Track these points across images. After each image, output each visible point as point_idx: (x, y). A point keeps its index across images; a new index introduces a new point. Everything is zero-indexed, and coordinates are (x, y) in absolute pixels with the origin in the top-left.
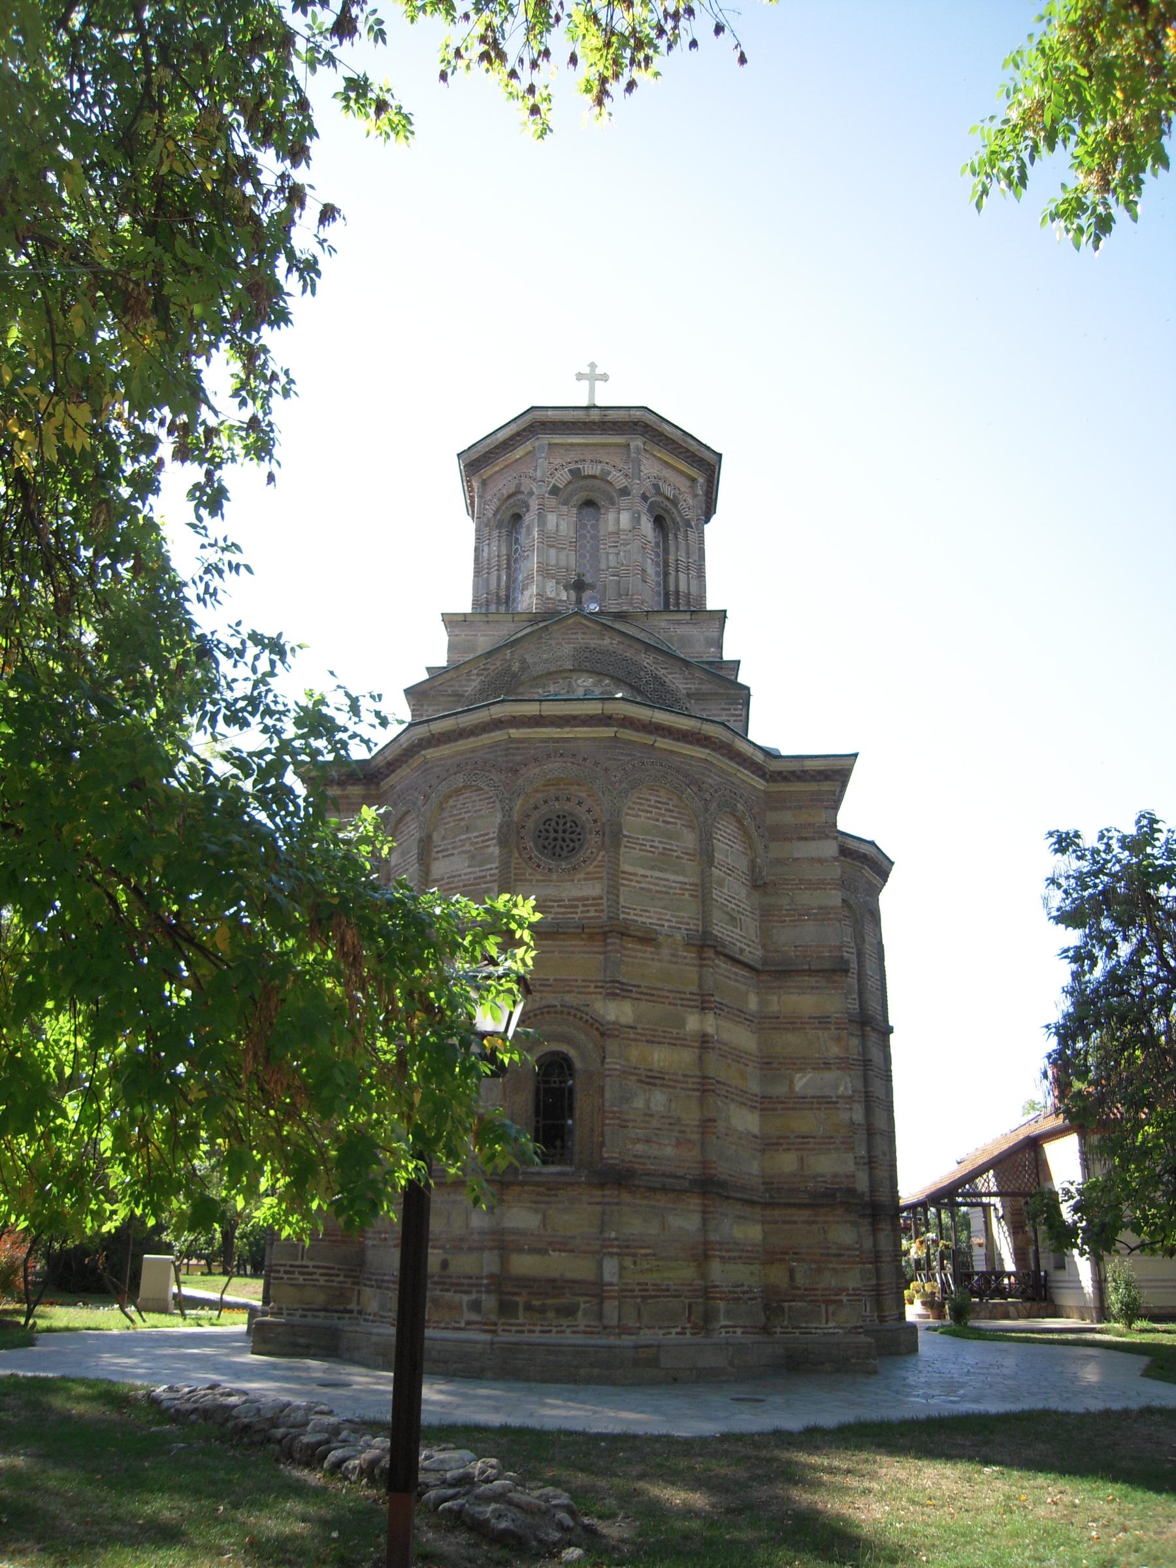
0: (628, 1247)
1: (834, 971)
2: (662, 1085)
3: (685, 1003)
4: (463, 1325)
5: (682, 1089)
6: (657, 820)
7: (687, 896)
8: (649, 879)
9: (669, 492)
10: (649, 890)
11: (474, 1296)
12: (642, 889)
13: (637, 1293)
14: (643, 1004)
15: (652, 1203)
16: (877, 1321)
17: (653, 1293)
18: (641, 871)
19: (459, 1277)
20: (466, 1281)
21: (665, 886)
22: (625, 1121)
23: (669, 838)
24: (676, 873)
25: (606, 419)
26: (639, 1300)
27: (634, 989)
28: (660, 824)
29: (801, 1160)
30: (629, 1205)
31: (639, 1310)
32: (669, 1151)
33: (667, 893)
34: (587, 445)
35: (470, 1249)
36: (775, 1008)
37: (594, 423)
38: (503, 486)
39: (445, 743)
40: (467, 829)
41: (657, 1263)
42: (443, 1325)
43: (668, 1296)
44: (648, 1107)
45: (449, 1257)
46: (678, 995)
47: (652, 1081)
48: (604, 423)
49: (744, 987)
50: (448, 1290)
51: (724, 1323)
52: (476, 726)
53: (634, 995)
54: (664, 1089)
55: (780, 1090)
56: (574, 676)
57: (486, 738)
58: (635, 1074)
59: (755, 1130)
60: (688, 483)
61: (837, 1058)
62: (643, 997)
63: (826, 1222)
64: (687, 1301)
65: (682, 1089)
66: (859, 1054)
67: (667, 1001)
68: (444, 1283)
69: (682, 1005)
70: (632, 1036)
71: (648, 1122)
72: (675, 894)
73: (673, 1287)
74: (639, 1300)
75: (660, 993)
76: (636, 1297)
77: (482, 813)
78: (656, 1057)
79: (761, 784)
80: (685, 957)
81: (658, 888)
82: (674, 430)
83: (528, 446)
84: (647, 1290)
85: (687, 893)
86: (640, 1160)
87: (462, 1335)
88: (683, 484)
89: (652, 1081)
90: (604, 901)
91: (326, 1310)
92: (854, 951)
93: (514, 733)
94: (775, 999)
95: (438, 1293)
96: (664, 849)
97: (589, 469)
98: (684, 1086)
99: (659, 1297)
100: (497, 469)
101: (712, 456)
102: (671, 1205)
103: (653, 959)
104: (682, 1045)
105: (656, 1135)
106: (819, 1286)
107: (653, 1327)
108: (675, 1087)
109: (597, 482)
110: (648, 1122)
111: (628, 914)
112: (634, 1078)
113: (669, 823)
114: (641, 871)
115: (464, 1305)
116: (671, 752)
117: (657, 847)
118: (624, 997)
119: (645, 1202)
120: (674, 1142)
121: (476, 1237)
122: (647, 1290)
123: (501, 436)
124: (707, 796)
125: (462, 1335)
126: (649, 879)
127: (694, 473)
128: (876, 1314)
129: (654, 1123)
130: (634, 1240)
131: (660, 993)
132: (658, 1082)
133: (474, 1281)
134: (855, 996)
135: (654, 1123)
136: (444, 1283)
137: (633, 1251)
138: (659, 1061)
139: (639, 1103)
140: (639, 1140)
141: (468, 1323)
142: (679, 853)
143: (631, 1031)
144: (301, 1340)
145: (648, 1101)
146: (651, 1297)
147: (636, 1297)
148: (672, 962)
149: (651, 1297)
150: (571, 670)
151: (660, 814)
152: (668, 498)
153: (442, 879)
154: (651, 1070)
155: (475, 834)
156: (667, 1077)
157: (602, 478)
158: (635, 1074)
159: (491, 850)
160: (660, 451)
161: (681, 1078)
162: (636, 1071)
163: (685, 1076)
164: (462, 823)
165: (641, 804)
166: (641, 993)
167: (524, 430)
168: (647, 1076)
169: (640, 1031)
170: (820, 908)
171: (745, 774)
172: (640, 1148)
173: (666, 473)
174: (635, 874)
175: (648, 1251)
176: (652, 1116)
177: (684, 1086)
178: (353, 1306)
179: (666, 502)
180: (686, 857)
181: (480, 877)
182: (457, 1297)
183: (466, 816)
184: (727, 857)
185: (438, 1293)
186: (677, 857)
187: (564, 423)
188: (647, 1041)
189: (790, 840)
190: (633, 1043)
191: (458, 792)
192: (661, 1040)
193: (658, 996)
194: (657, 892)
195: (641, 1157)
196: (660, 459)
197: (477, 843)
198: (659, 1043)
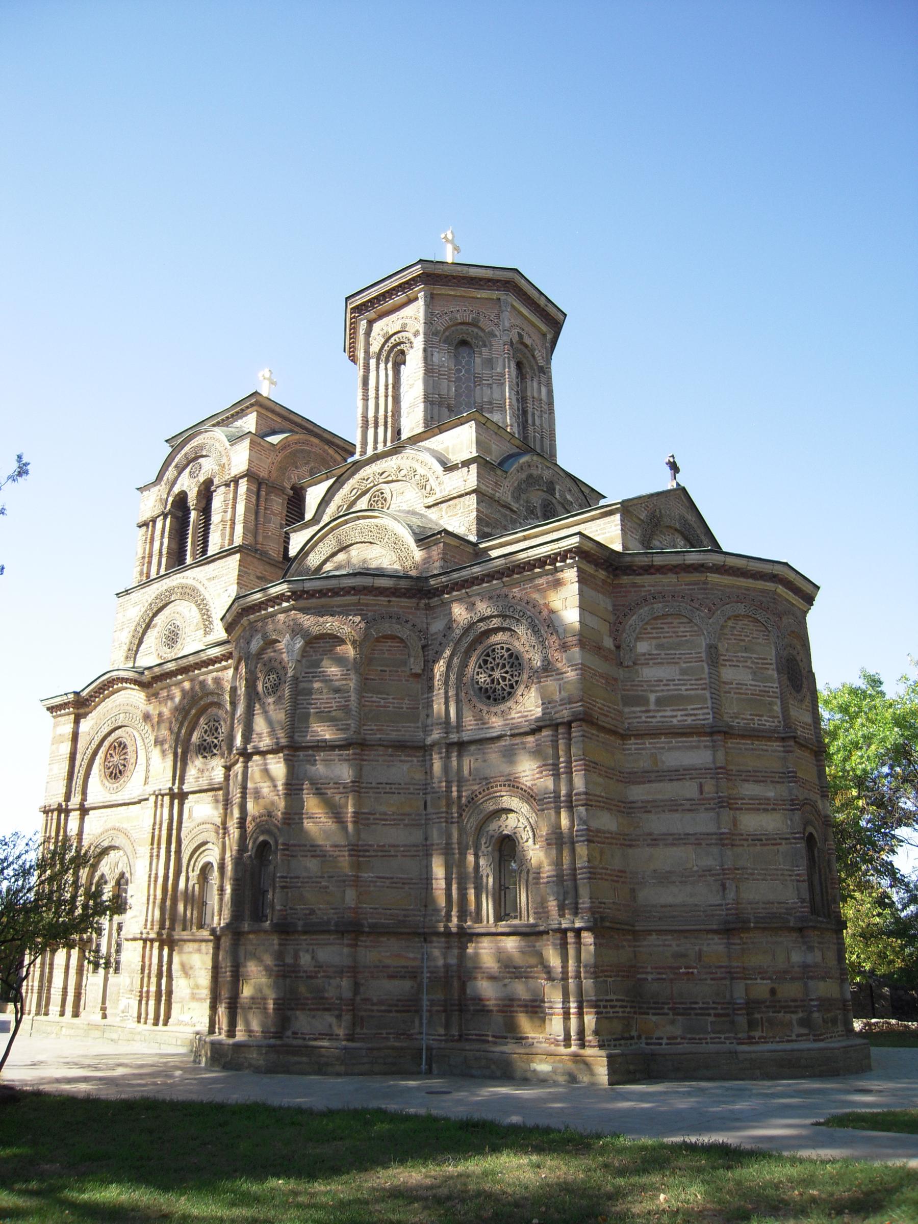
4: (794, 1037)
11: (800, 1015)
19: (786, 1001)
20: (793, 1004)
25: (547, 308)
34: (526, 318)
35: (792, 979)
38: (463, 313)
39: (730, 575)
40: (746, 650)
42: (778, 1039)
45: (776, 986)
48: (544, 310)
50: (779, 1012)
52: (759, 572)
56: (677, 535)
57: (760, 584)
68: (775, 1006)
77: (760, 640)
83: (495, 294)
87: (795, 1046)
90: (812, 728)
91: (623, 1038)
93: (781, 589)
95: (771, 1014)
97: (528, 341)
100: (452, 293)
109: (526, 351)
115: (795, 1022)
121: (796, 969)
123: (473, 272)
125: (795, 1046)
133: (798, 1003)
136: (775, 1006)
141: (798, 1036)
144: (631, 1067)
150: (676, 530)
153: (732, 684)
155: (755, 656)
157: (532, 351)
159: (770, 672)
164: (742, 644)
167: (498, 281)
178: (634, 1033)
181: (765, 691)
182: (788, 1016)
183: (747, 639)
185: (771, 1014)
187: (525, 294)
191: (737, 617)
197: (758, 663)
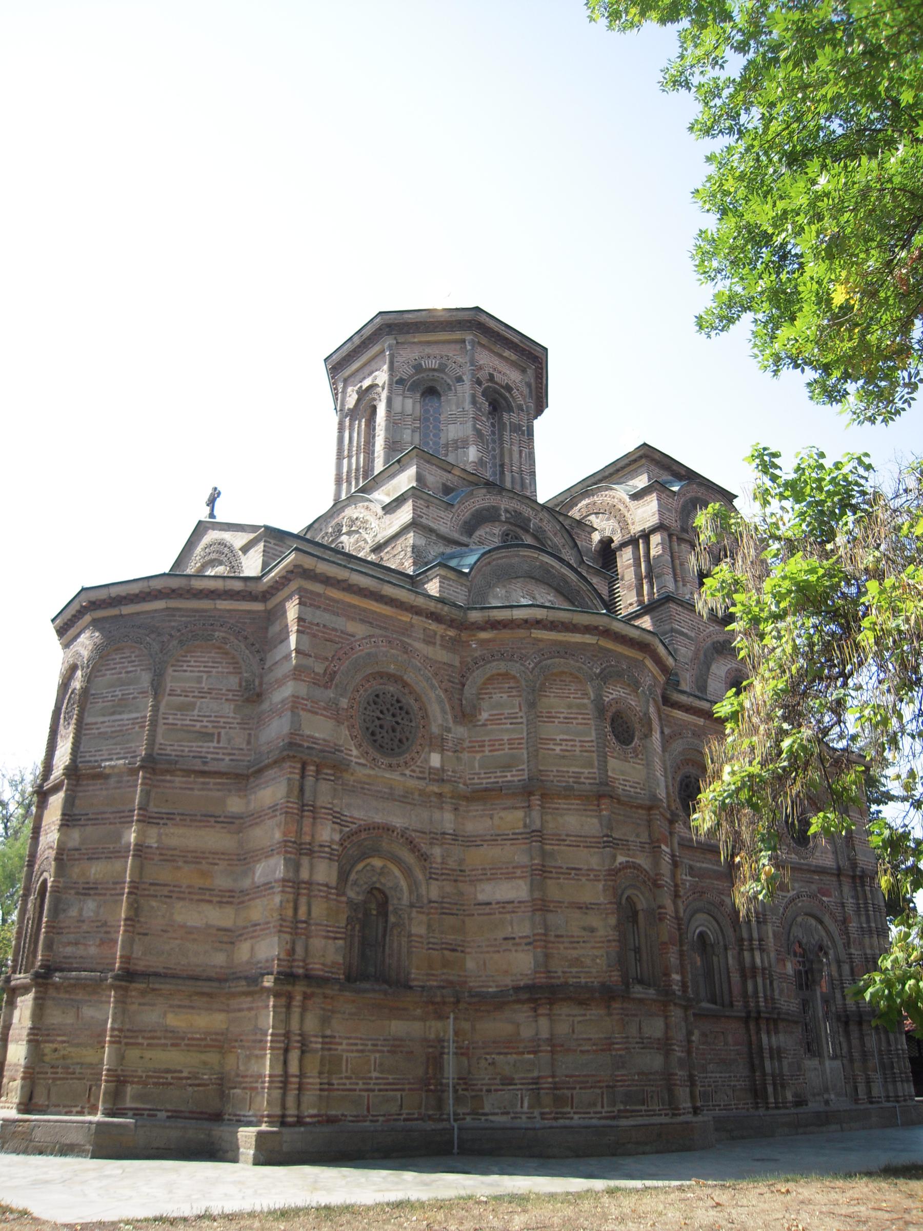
0: (48, 1035)
1: (283, 759)
2: (95, 894)
3: (123, 820)
5: (112, 895)
6: (121, 673)
7: (137, 727)
8: (107, 724)
9: (433, 364)
10: (106, 733)
12: (100, 733)
13: (49, 1075)
14: (89, 829)
15: (72, 997)
16: (538, 1118)
17: (62, 1076)
18: (101, 719)
21: (119, 725)
22: (61, 928)
23: (129, 684)
24: (130, 712)
26: (50, 1081)
27: (83, 818)
28: (123, 675)
29: (252, 949)
30: (54, 999)
31: (49, 1090)
32: (93, 950)
33: (121, 731)
36: (252, 806)
37: (359, 346)
41: (69, 1049)
43: (72, 1079)
44: (81, 915)
46: (118, 815)
47: (87, 891)
49: (219, 794)
51: (129, 1104)
53: (82, 822)
54: (96, 897)
55: (246, 883)
58: (74, 888)
59: (228, 923)
60: (458, 347)
61: (279, 843)
62: (90, 822)
63: (258, 1008)
64: (89, 1083)
65: (112, 895)
66: (525, 826)
67: (107, 821)
69: (120, 823)
70: (77, 857)
71: (79, 927)
72: (127, 730)
73: (78, 1071)
74: (50, 1081)
75: (104, 816)
76: (49, 1079)
78: (93, 871)
79: (258, 607)
80: (128, 781)
81: (113, 729)
82: (419, 314)
84: (57, 1073)
85: (137, 727)
86: (67, 961)
88: (451, 351)
89: (87, 891)
92: (524, 720)
94: (253, 797)
96: (123, 695)
98: (113, 892)
99: (67, 1079)
101: (467, 313)
102: (87, 998)
103: (102, 789)
104: (116, 857)
105: (84, 938)
106: (249, 1073)
107: (58, 1106)
108: (105, 895)
110: (79, 927)
111: (85, 757)
112: (73, 892)
113: (130, 672)
114: (101, 719)
116: (138, 614)
117: (117, 696)
118: (74, 826)
119: (67, 996)
120: (98, 942)
122: (57, 1073)
124: (165, 638)
126: (107, 724)
127: (457, 335)
128: (536, 1113)
129: (85, 927)
130: (54, 1029)
131: (104, 816)
132: (92, 892)
134: (524, 767)
135: (85, 927)
137: (52, 1038)
138: (95, 874)
139: (73, 912)
140: (69, 944)
142: (136, 695)
143: (76, 853)
145: (81, 910)
146: (60, 1079)
147: (49, 1079)
148: (116, 788)
149: (60, 1079)
151: (124, 668)
152: (434, 370)
154: (88, 883)
156: (99, 886)
158: (74, 888)
160: (414, 337)
161: (111, 886)
162: (76, 886)
163: (114, 883)
165: (107, 665)
166: (89, 819)
168: (83, 888)
169: (84, 851)
170: (282, 701)
171: (224, 605)
172: (69, 950)
173: (428, 350)
174: (96, 723)
175: (64, 1038)
176: (83, 921)
177: (113, 892)
179: (431, 374)
180: (141, 696)
184: (200, 682)
186: (134, 698)
188: (88, 859)
189: (275, 647)
190: (77, 862)
192: (100, 856)
193: (102, 819)
194: (112, 732)
195: (69, 957)
196: (420, 342)
198: (98, 859)
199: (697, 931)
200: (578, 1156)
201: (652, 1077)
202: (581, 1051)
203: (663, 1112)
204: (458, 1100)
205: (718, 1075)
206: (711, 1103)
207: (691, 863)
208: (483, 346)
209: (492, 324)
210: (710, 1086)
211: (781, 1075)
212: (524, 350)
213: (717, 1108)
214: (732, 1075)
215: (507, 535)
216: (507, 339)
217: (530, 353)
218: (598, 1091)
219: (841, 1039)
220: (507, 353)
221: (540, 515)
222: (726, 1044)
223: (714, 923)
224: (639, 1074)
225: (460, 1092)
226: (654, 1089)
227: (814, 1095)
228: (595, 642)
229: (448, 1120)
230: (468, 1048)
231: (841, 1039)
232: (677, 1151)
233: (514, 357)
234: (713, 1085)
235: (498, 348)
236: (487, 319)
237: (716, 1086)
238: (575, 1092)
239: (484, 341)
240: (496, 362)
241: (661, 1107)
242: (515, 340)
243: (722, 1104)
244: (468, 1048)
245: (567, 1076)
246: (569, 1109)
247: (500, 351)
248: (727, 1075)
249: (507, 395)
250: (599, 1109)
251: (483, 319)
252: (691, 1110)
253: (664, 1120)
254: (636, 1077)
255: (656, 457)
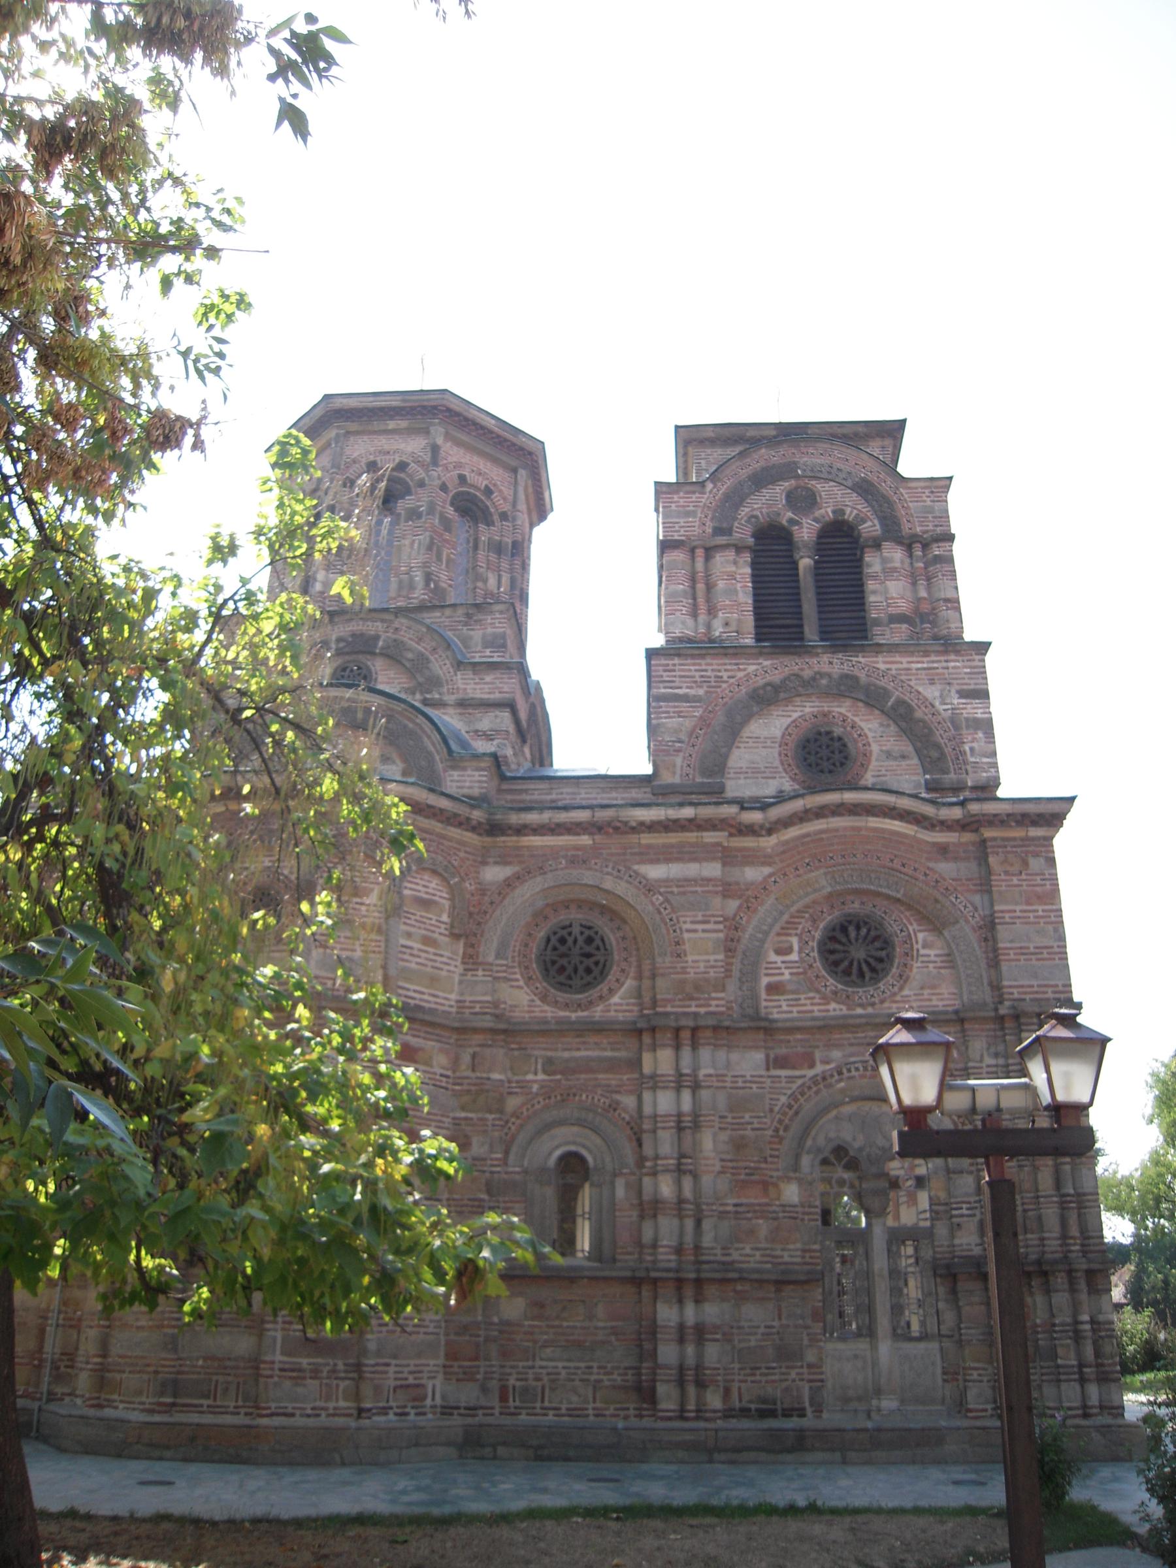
199: (558, 1153)
200: (87, 1453)
201: (228, 1363)
202: (138, 1328)
203: (243, 1411)
204: (58, 1378)
205: (560, 1364)
206: (538, 1405)
207: (549, 1054)
208: (357, 433)
209: (353, 403)
210: (538, 1379)
211: (699, 1367)
212: (413, 408)
213: (551, 1412)
214: (595, 1365)
215: (344, 670)
216: (382, 409)
217: (424, 407)
218: (145, 1377)
219: (941, 1305)
220: (391, 425)
221: (396, 625)
222: (591, 1317)
223: (593, 1136)
224: (205, 1359)
225: (62, 1369)
226: (230, 1379)
227: (846, 1400)
228: (223, 809)
229: (40, 1399)
230: (80, 1320)
231: (941, 1305)
232: (221, 1461)
233: (403, 424)
234: (546, 1378)
235: (376, 425)
236: (345, 401)
237: (553, 1381)
238: (124, 1376)
239: (353, 426)
240: (383, 442)
241: (240, 1403)
242: (394, 404)
243: (564, 1406)
244: (80, 1320)
245: (121, 1357)
246: (115, 1397)
247: (382, 427)
248: (582, 1365)
249: (402, 475)
250: (144, 1399)
251: (338, 404)
252: (355, 1412)
253: (240, 1420)
254: (200, 1362)
255: (711, 434)
